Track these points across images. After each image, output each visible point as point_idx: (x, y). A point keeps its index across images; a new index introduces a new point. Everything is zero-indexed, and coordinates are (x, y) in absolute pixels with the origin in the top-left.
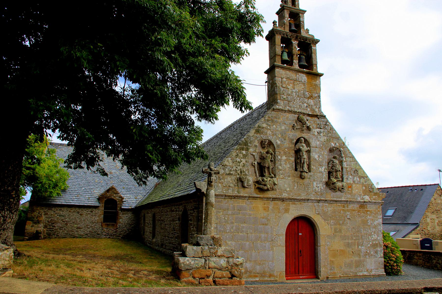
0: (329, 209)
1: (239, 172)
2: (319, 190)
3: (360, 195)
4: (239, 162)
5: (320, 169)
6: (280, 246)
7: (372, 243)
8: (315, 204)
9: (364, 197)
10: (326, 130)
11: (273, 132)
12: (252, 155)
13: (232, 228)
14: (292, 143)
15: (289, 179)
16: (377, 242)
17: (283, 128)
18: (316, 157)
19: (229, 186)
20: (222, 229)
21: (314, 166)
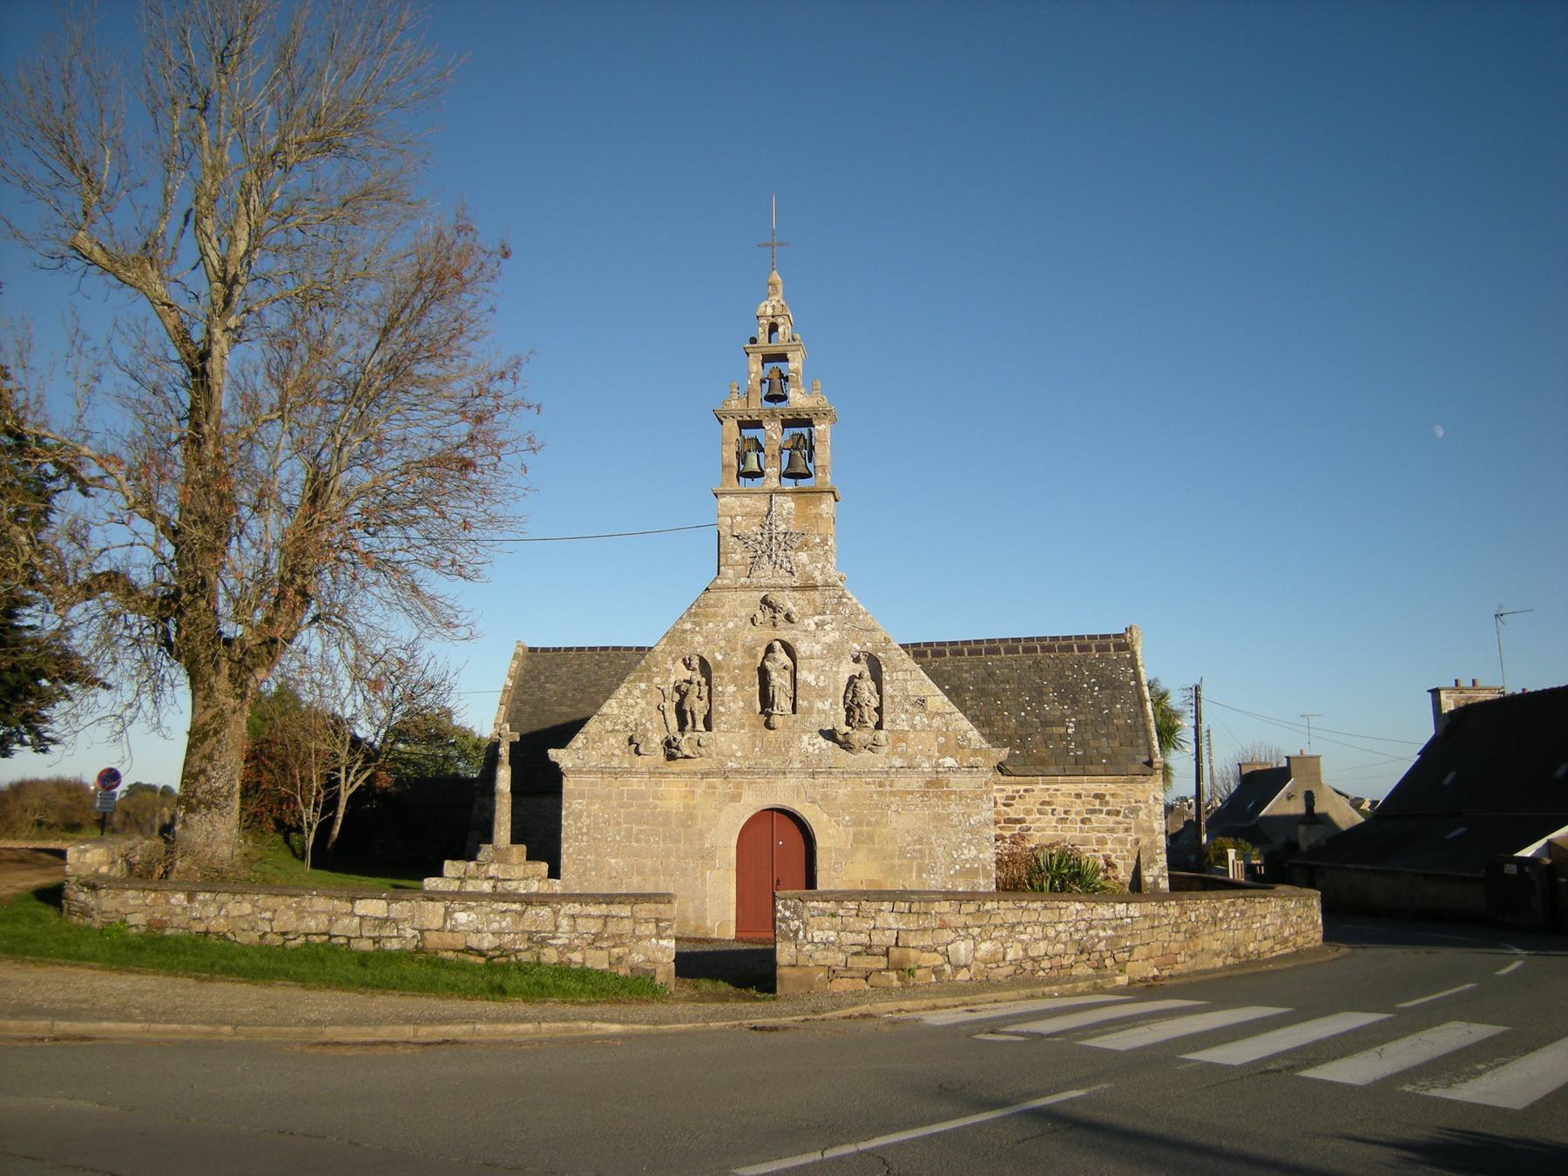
0: (842, 791)
1: (631, 725)
2: (817, 752)
3: (930, 757)
4: (632, 706)
9: (940, 761)
10: (840, 616)
13: (618, 833)
15: (742, 731)
18: (811, 678)
19: (613, 754)
20: (599, 836)
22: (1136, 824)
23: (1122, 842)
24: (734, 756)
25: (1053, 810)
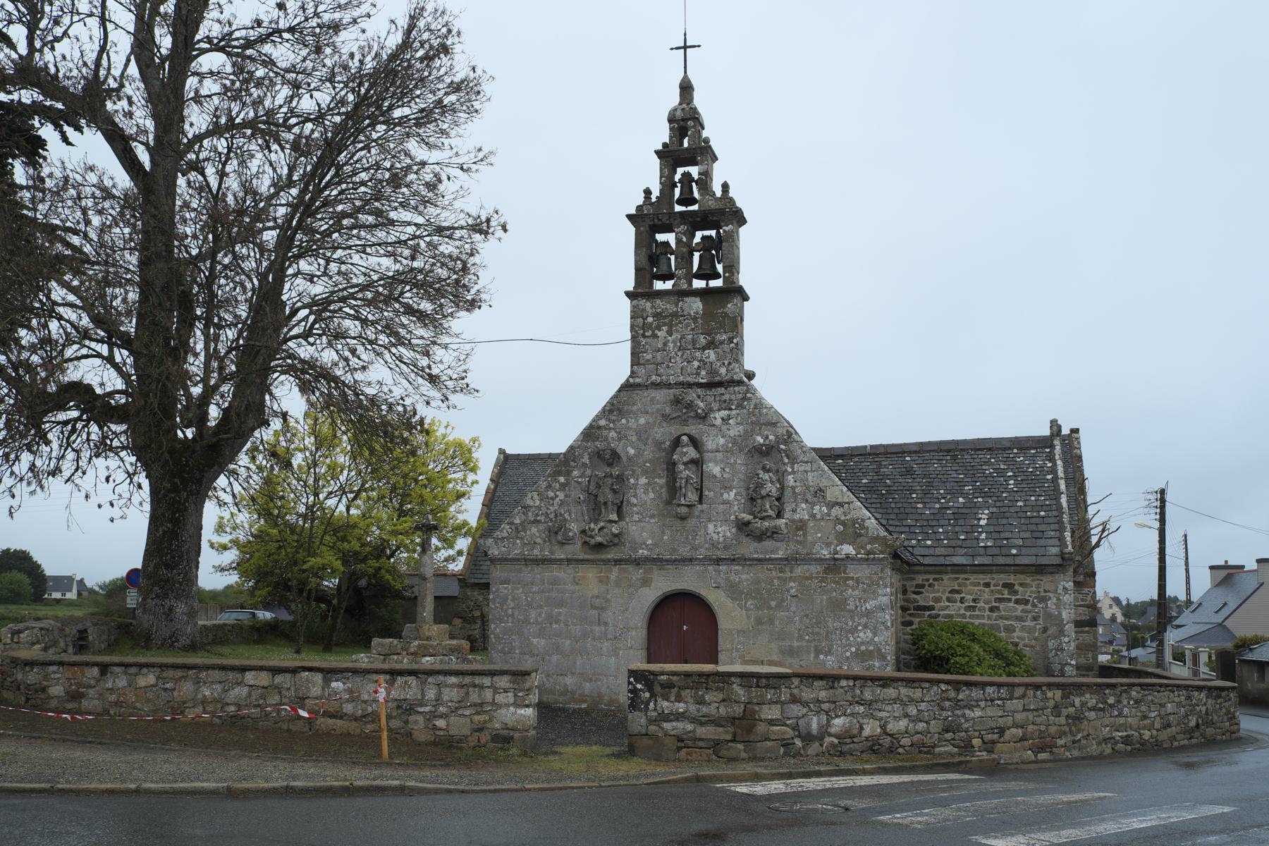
0: (744, 576)
1: (552, 516)
2: (721, 540)
4: (553, 499)
5: (725, 496)
6: (631, 648)
7: (857, 650)
8: (711, 568)
9: (838, 548)
11: (620, 433)
12: (577, 482)
13: (540, 615)
14: (660, 449)
15: (653, 521)
16: (871, 648)
17: (642, 421)
19: (535, 543)
21: (709, 490)
23: (1030, 630)
24: (645, 543)
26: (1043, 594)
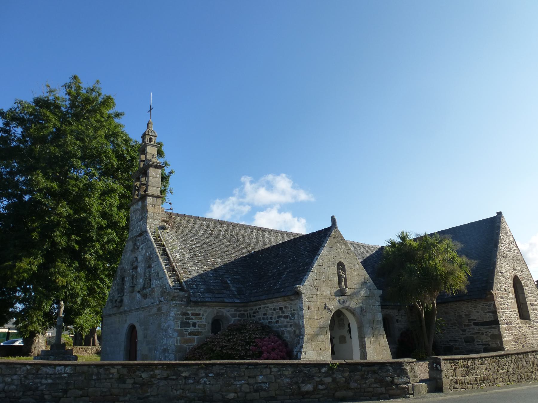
22: (294, 322)
25: (267, 317)
26: (293, 312)
